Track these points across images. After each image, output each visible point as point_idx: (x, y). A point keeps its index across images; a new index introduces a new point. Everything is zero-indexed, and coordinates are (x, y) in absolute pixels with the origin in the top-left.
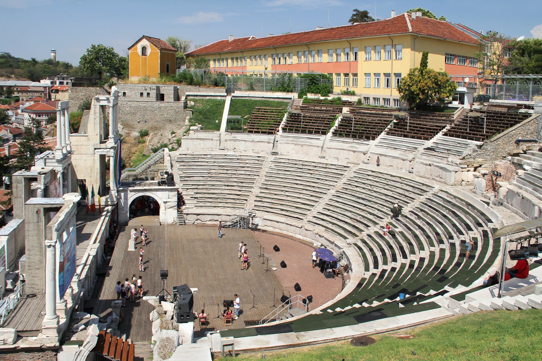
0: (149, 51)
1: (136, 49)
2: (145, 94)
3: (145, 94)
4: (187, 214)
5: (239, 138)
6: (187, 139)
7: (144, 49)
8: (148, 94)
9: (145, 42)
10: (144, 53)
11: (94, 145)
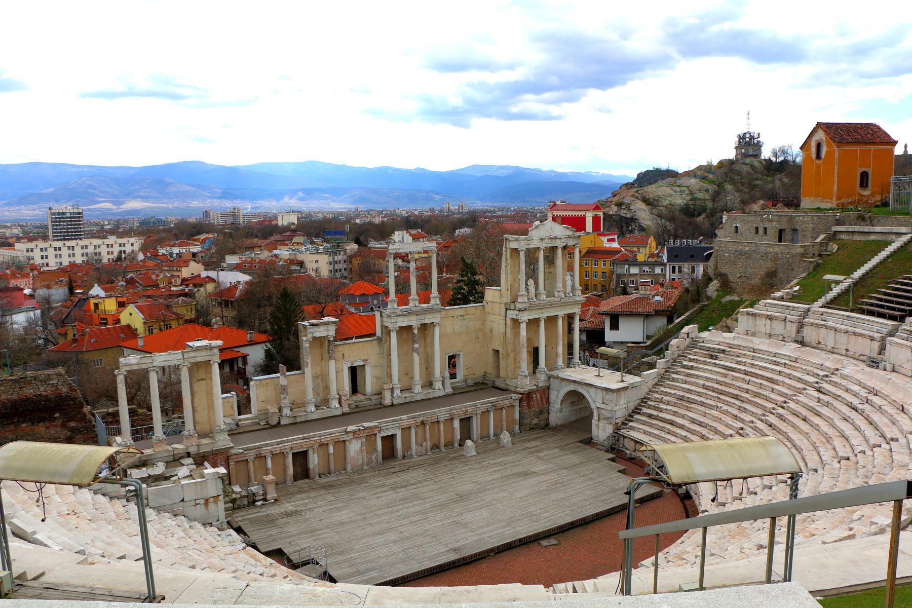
0: (824, 150)
1: (810, 147)
2: (761, 231)
3: (761, 231)
4: (624, 437)
5: (830, 324)
6: (748, 314)
7: (819, 146)
8: (765, 228)
9: (821, 135)
10: (818, 156)
11: (505, 304)
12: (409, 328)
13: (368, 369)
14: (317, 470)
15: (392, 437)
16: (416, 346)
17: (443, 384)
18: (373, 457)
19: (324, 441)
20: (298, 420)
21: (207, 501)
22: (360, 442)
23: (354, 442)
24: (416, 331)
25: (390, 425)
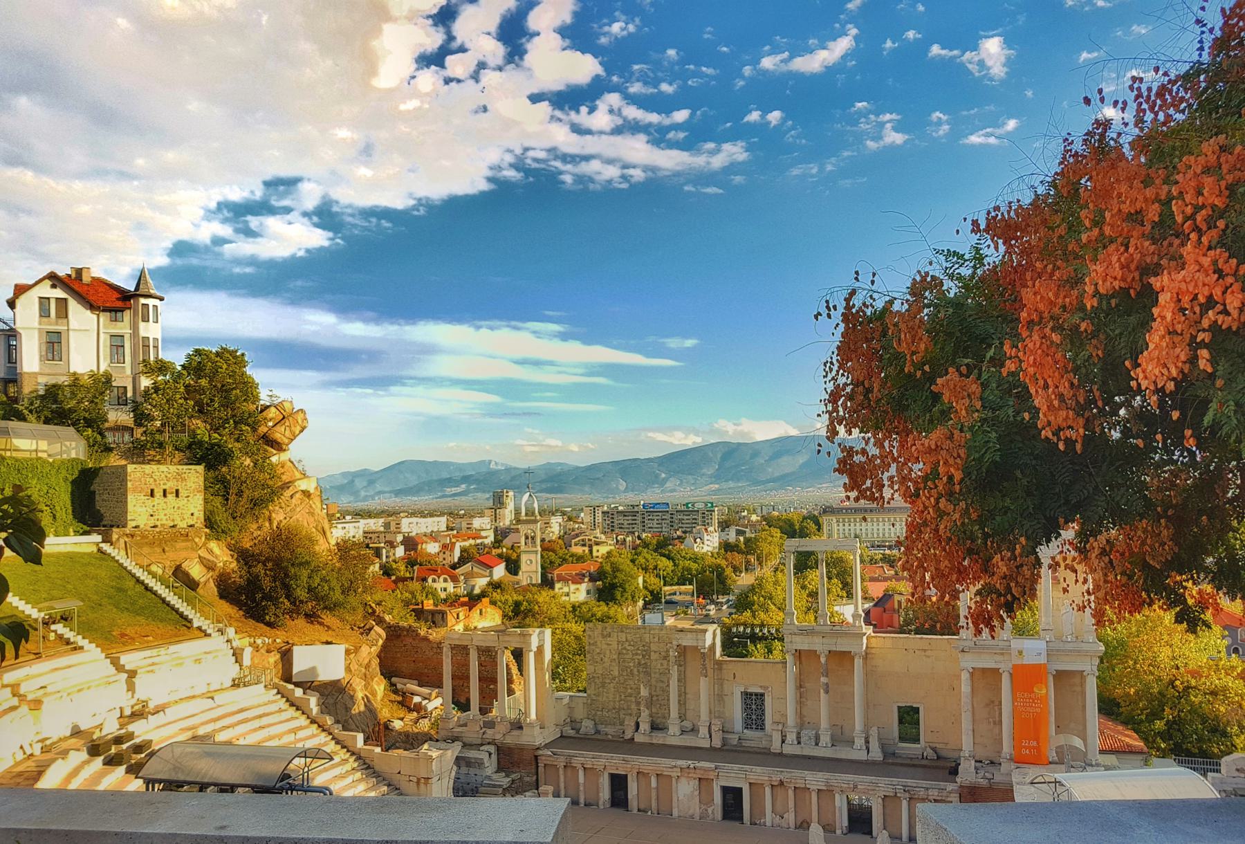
12: (813, 654)
13: (768, 700)
14: (635, 804)
15: (739, 791)
16: (823, 680)
17: (867, 742)
18: (710, 811)
19: (645, 769)
20: (654, 741)
21: (418, 783)
22: (692, 783)
23: (683, 781)
24: (823, 660)
25: (734, 775)
